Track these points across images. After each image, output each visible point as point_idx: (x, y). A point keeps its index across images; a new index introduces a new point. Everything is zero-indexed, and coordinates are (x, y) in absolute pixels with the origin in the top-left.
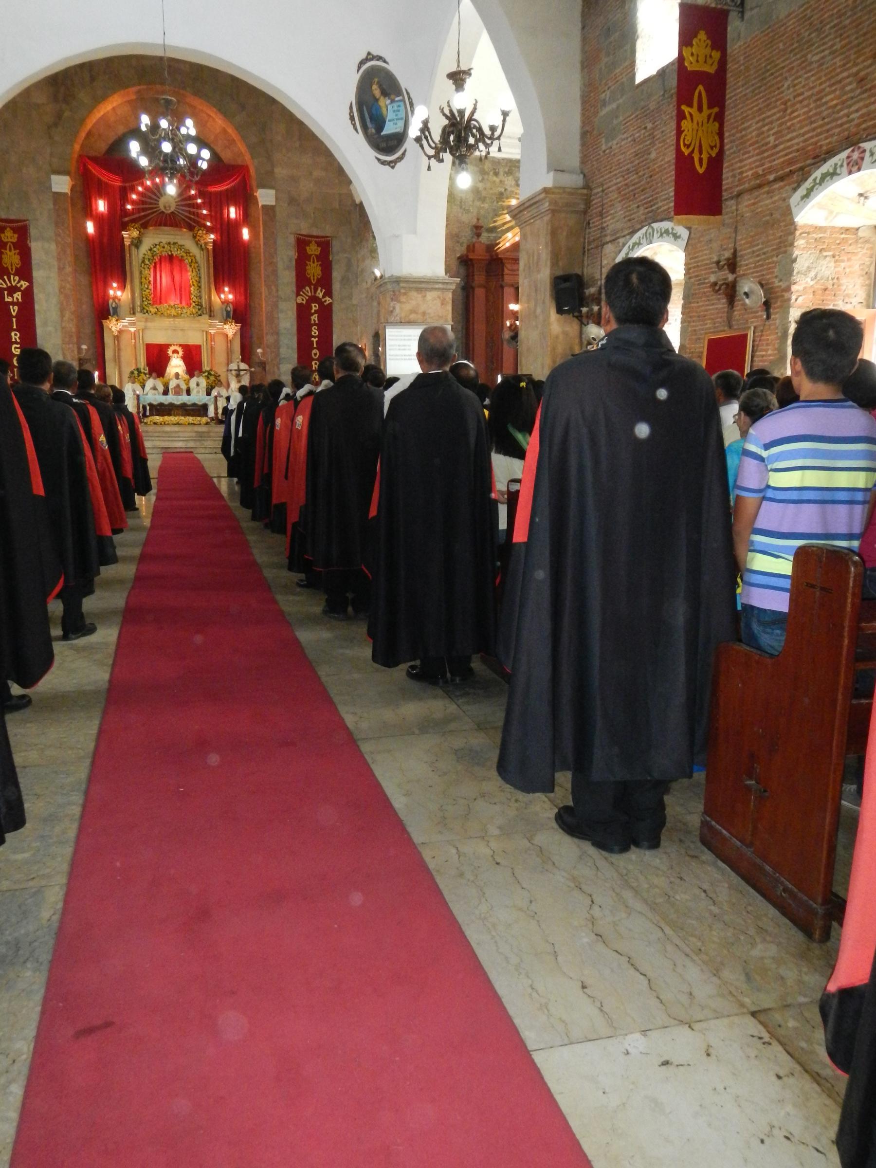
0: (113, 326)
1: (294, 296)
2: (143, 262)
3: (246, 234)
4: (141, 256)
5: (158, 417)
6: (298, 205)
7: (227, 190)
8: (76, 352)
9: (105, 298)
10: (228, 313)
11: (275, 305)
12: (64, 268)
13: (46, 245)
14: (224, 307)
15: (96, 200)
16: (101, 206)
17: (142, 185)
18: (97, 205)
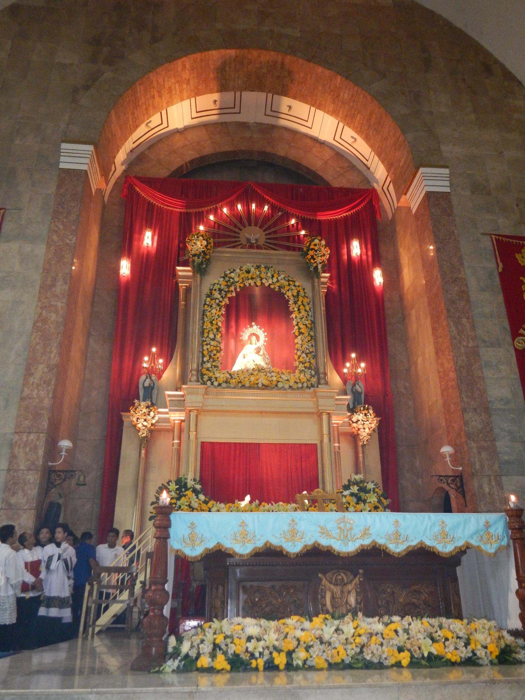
0: (141, 418)
1: (509, 338)
2: (210, 295)
3: (378, 277)
4: (206, 290)
5: (252, 626)
6: (489, 194)
7: (346, 218)
8: (41, 452)
9: (135, 370)
10: (356, 395)
11: (474, 353)
12: (53, 285)
13: (28, 248)
14: (349, 387)
15: (141, 233)
16: (148, 239)
17: (215, 212)
18: (141, 240)
